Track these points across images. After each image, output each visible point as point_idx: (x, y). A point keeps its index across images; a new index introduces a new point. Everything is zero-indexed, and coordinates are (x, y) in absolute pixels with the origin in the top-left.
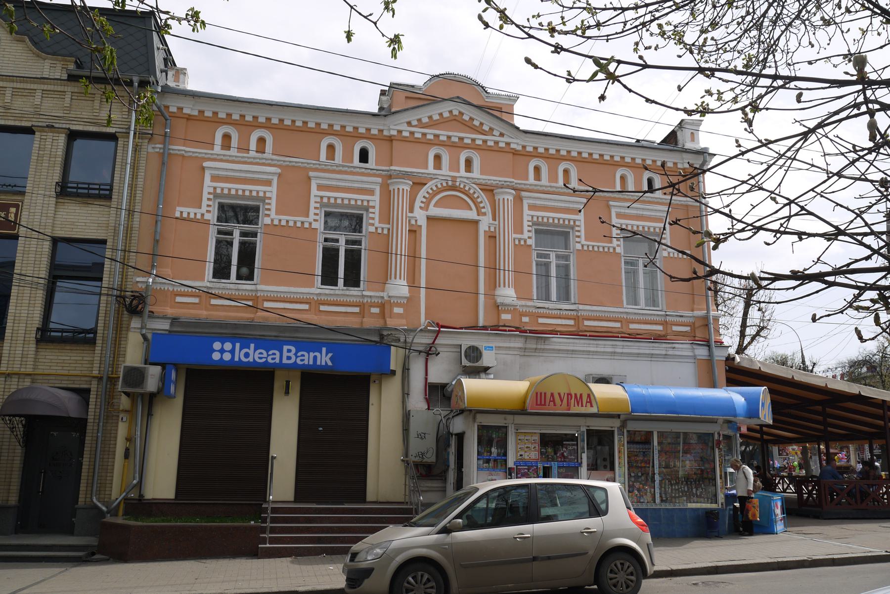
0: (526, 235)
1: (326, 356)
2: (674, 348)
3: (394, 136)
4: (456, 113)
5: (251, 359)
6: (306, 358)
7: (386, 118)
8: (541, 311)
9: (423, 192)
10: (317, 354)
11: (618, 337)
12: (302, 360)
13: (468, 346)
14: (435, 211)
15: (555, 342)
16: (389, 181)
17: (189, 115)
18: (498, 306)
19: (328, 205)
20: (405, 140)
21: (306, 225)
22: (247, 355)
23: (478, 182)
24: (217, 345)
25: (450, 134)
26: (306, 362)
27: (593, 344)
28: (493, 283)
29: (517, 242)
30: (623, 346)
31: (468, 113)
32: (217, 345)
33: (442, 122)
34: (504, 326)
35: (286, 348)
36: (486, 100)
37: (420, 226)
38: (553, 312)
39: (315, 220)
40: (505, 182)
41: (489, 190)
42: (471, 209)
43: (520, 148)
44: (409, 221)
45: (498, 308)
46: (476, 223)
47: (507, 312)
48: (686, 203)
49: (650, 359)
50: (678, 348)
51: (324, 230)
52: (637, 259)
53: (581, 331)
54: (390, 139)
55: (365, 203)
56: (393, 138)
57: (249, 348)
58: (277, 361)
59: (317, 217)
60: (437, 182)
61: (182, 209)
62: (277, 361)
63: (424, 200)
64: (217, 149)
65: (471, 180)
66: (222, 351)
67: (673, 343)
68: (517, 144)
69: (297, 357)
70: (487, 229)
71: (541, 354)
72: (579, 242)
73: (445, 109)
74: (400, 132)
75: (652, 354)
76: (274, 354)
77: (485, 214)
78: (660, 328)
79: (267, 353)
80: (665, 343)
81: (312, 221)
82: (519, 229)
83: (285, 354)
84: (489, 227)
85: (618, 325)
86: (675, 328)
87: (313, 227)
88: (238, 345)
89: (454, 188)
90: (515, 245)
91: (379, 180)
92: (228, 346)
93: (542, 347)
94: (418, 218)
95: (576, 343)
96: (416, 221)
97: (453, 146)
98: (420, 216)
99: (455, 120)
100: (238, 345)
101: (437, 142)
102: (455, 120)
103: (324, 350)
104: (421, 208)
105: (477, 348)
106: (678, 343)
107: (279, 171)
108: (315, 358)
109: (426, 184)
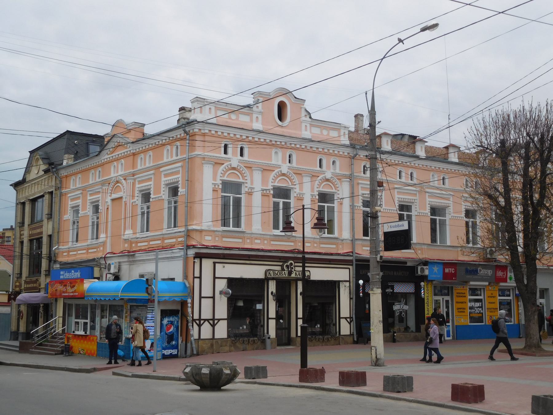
0: (136, 198)
14: (114, 196)
17: (66, 175)
43: (134, 151)
46: (121, 198)
49: (168, 260)
50: (175, 252)
67: (173, 250)
75: (168, 257)
78: (174, 240)
80: (170, 250)
82: (133, 196)
83: (72, 274)
85: (159, 242)
89: (118, 182)
98: (109, 199)
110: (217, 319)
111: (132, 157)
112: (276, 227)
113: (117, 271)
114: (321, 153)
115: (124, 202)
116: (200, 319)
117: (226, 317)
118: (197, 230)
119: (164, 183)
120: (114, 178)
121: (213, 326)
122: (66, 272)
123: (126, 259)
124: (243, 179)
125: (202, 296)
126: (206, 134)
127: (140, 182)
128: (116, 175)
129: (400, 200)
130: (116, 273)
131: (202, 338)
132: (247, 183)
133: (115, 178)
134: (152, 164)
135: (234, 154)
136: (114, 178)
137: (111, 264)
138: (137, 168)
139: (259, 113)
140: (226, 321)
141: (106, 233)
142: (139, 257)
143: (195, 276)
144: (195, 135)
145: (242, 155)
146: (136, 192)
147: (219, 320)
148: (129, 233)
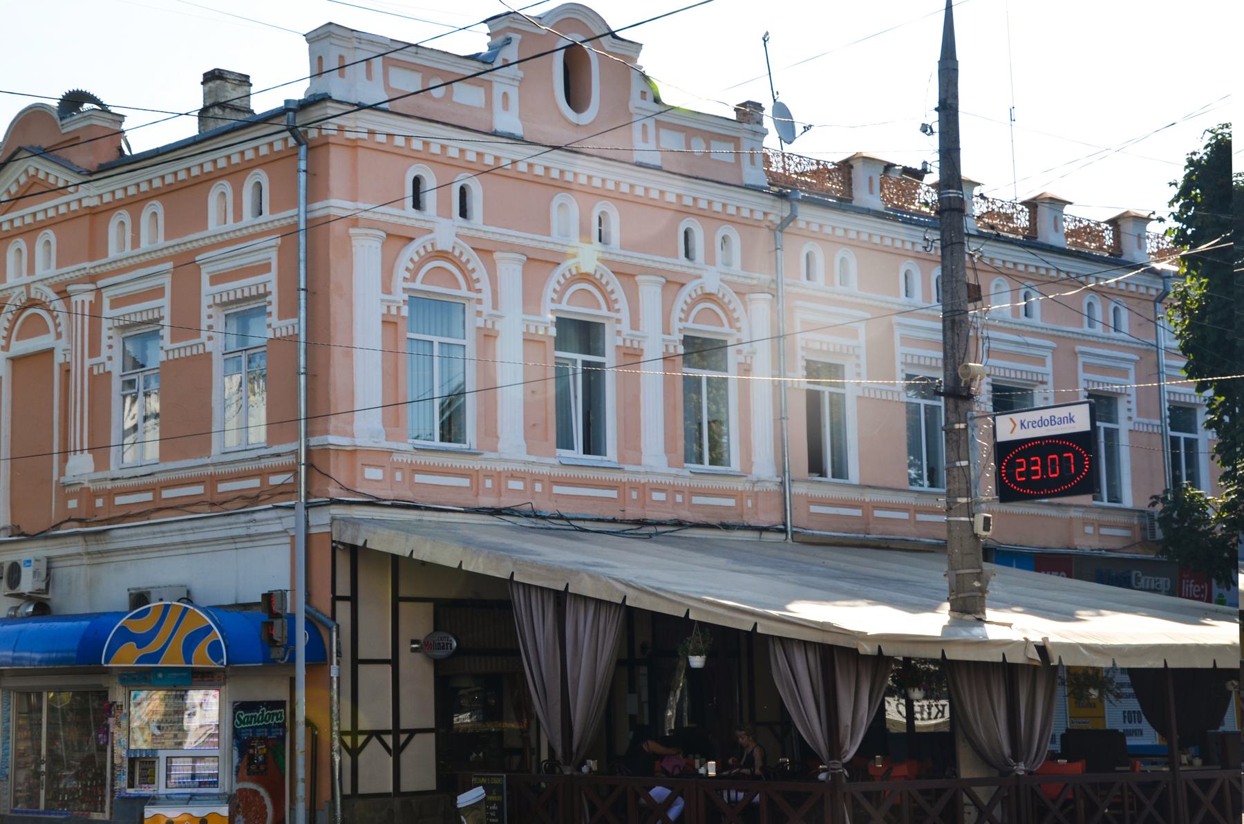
0: (105, 352)
4: (32, 172)
8: (118, 484)
40: (79, 270)
41: (64, 294)
42: (48, 331)
46: (50, 352)
49: (233, 546)
52: (239, 354)
67: (253, 512)
75: (232, 538)
82: (94, 350)
86: (275, 480)
93: (101, 548)
105: (16, 563)
106: (259, 511)
110: (405, 731)
111: (86, 220)
112: (565, 442)
113: (43, 586)
114: (691, 211)
115: (61, 365)
116: (355, 732)
117: (432, 724)
118: (339, 450)
119: (211, 302)
120: (17, 291)
121: (396, 752)
123: (77, 546)
124: (469, 289)
125: (361, 656)
126: (360, 143)
127: (116, 303)
128: (26, 279)
129: (909, 360)
130: (39, 591)
131: (361, 790)
132: (479, 301)
134: (161, 242)
135: (444, 211)
136: (17, 291)
137: (22, 564)
138: (106, 255)
139: (511, 82)
140: (432, 737)
142: (122, 536)
143: (338, 593)
144: (328, 143)
145: (464, 213)
146: (105, 333)
147: (412, 733)
148: (81, 466)
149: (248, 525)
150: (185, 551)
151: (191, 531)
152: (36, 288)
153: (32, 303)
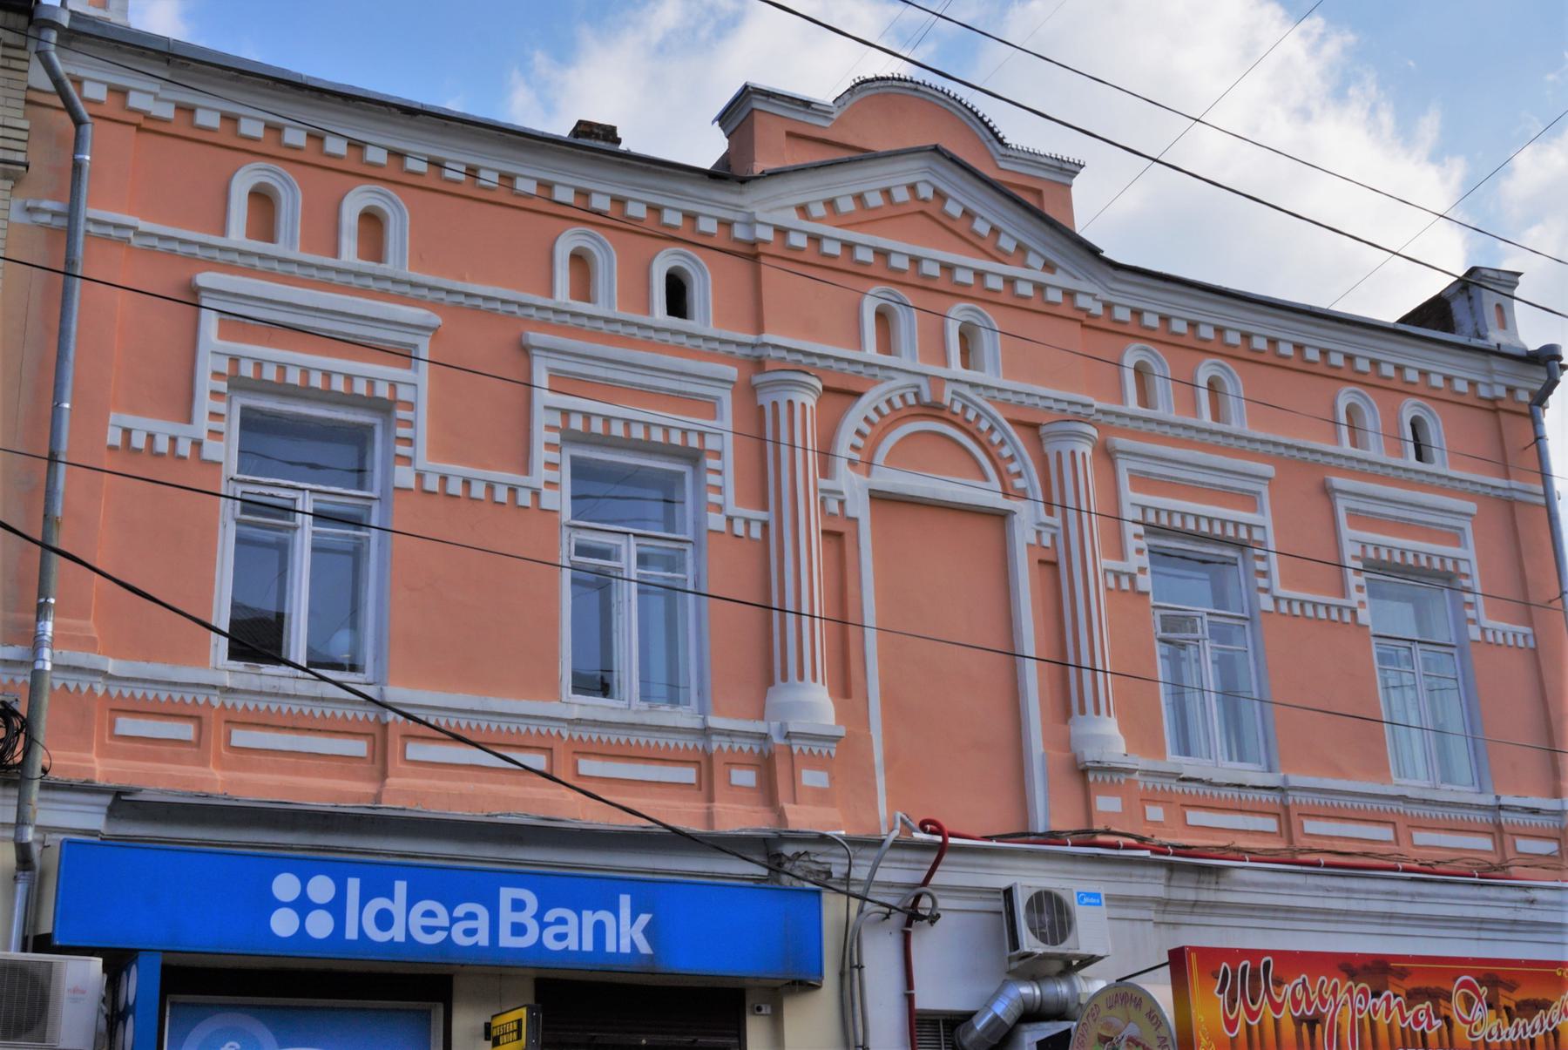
1: (633, 921)
2: (1532, 902)
3: (766, 242)
4: (925, 192)
5: (397, 934)
6: (571, 929)
7: (745, 188)
9: (856, 416)
10: (606, 916)
11: (1396, 869)
12: (560, 937)
13: (1035, 891)
15: (1244, 883)
16: (758, 379)
17: (147, 116)
18: (1084, 772)
19: (586, 439)
20: (792, 258)
21: (525, 498)
22: (384, 919)
23: (1000, 396)
24: (285, 886)
25: (919, 251)
26: (572, 944)
27: (1340, 889)
28: (1066, 706)
29: (1112, 583)
30: (1412, 895)
31: (960, 197)
32: (285, 886)
33: (890, 214)
34: (1108, 832)
35: (507, 895)
36: (1002, 165)
37: (855, 520)
38: (1224, 792)
39: (549, 484)
42: (986, 478)
43: (1097, 309)
44: (823, 501)
45: (1084, 774)
46: (1002, 517)
47: (1112, 789)
48: (1508, 494)
49: (1475, 934)
50: (1544, 903)
51: (574, 517)
53: (1301, 851)
54: (752, 253)
55: (694, 442)
56: (761, 249)
57: (391, 896)
58: (483, 939)
59: (553, 476)
60: (891, 391)
61: (128, 420)
62: (483, 939)
63: (860, 442)
64: (237, 233)
65: (981, 390)
66: (303, 906)
68: (1093, 296)
69: (543, 926)
70: (1034, 540)
71: (1205, 920)
72: (1266, 591)
73: (899, 177)
74: (782, 231)
75: (1483, 921)
76: (471, 916)
77: (1022, 495)
79: (450, 912)
81: (542, 487)
83: (507, 917)
84: (1039, 533)
85: (1385, 833)
86: (1525, 845)
87: (545, 504)
88: (354, 885)
89: (934, 410)
90: (1108, 589)
91: (732, 372)
92: (321, 888)
94: (847, 495)
95: (1297, 886)
96: (842, 503)
97: (925, 286)
98: (852, 486)
99: (922, 212)
100: (354, 885)
101: (881, 269)
102: (922, 212)
103: (625, 901)
104: (852, 462)
107: (435, 320)
108: (599, 928)
109: (859, 395)
120: (902, 380)
122: (376, 886)
133: (923, 382)
141: (845, 686)
149: (1519, 905)
150: (1377, 929)
151: (1409, 899)
152: (954, 393)
153: (934, 410)
